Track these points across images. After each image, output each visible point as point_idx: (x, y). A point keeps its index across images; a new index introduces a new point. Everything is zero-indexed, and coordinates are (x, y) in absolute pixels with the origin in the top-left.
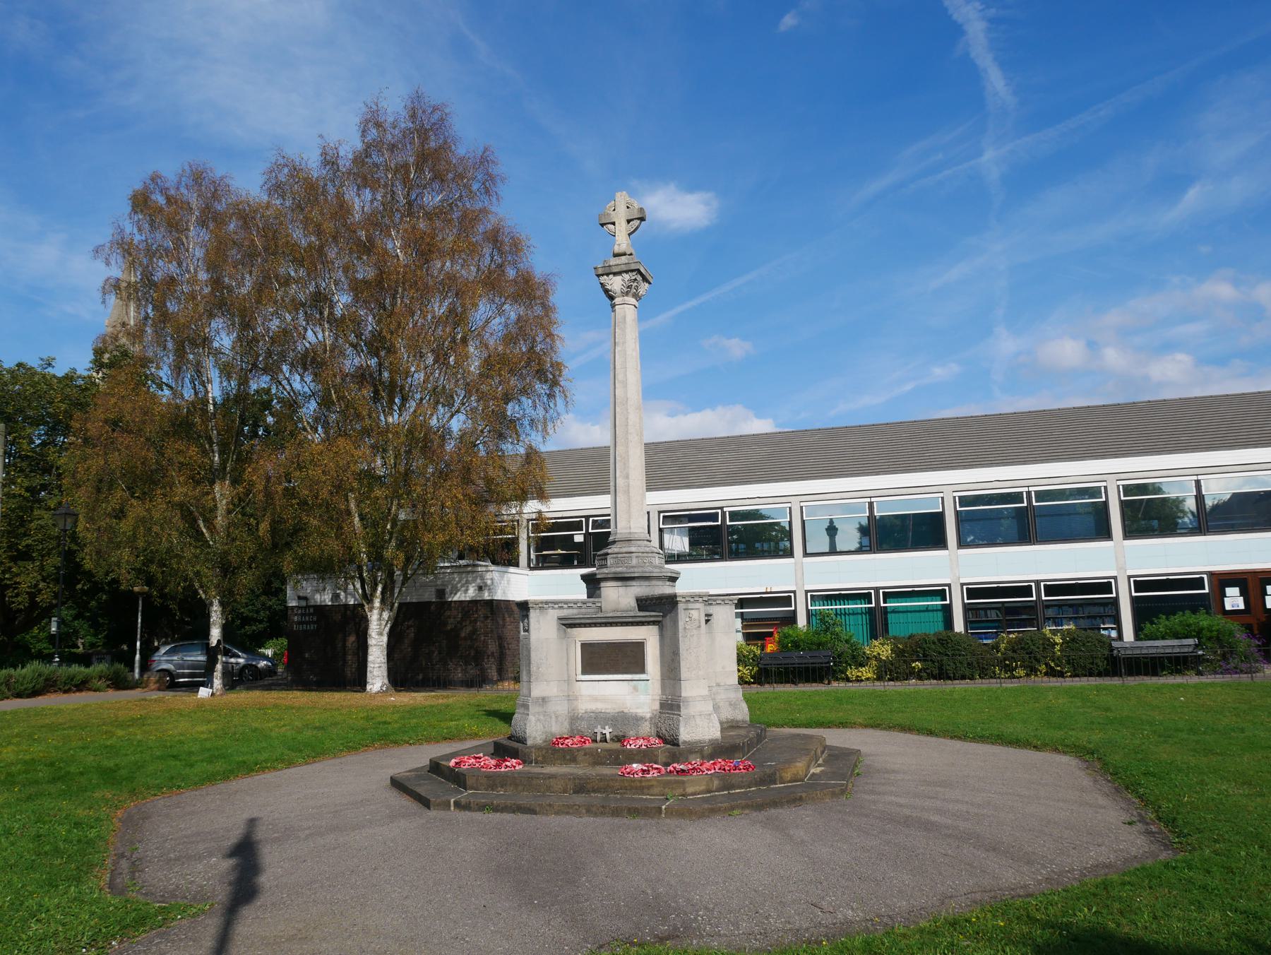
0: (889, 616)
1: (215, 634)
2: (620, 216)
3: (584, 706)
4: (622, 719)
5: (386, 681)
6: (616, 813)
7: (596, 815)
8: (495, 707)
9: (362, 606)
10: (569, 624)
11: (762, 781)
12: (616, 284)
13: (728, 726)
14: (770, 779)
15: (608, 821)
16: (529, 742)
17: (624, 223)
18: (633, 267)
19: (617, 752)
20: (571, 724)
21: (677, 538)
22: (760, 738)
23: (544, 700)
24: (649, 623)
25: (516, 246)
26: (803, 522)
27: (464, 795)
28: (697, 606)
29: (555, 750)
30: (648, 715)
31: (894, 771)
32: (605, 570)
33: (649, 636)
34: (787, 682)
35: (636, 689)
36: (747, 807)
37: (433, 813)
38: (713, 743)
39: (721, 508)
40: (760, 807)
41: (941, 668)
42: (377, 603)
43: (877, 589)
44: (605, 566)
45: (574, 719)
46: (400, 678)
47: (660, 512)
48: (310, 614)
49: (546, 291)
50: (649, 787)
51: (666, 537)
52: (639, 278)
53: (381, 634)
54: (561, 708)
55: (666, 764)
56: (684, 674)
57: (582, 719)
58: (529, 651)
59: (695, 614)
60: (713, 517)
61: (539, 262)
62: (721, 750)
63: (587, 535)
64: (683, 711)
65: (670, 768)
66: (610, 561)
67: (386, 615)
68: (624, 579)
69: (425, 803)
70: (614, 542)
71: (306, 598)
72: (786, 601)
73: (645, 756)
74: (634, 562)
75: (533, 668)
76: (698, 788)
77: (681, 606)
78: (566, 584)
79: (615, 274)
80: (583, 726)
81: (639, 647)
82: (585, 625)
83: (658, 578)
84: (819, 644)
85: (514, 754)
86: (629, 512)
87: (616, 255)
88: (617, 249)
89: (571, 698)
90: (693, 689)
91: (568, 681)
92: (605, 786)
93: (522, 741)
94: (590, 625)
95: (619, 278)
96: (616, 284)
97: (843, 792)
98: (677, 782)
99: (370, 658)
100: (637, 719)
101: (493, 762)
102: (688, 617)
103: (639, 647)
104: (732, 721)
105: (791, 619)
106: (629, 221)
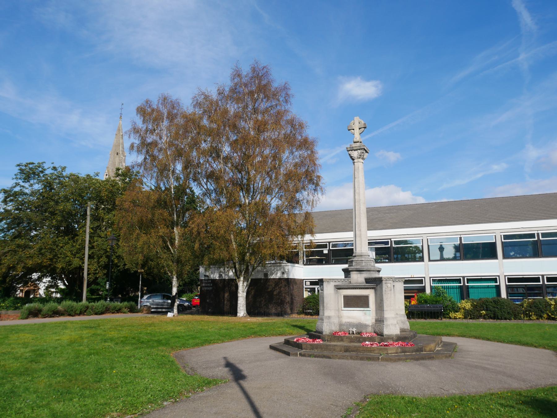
0: (470, 290)
1: (175, 291)
2: (356, 126)
3: (345, 320)
4: (360, 326)
5: (246, 312)
6: (362, 359)
7: (354, 360)
8: (294, 324)
9: (236, 280)
10: (338, 288)
11: (417, 351)
12: (355, 154)
13: (402, 330)
14: (420, 350)
15: (359, 362)
16: (324, 333)
17: (358, 129)
18: (362, 147)
19: (359, 338)
22: (415, 336)
23: (329, 317)
24: (370, 288)
25: (301, 126)
26: (428, 246)
27: (303, 351)
28: (390, 282)
29: (334, 336)
30: (371, 324)
31: (471, 351)
32: (352, 267)
33: (370, 293)
34: (422, 318)
35: (365, 314)
36: (412, 359)
37: (291, 357)
38: (397, 335)
39: (390, 239)
40: (417, 359)
41: (494, 314)
42: (242, 279)
43: (464, 277)
44: (352, 266)
45: (341, 325)
46: (252, 311)
48: (209, 283)
49: (313, 145)
50: (374, 350)
52: (364, 152)
53: (243, 292)
54: (336, 321)
55: (379, 343)
56: (385, 308)
57: (344, 325)
58: (323, 298)
59: (389, 285)
60: (387, 243)
61: (310, 133)
62: (399, 338)
63: (329, 250)
64: (385, 323)
65: (381, 344)
66: (354, 264)
67: (245, 284)
68: (360, 271)
69: (288, 354)
70: (355, 256)
71: (208, 276)
72: (421, 281)
73: (371, 339)
74: (364, 264)
75: (325, 305)
76: (393, 352)
77: (384, 282)
78: (333, 272)
79: (355, 150)
80: (344, 328)
81: (366, 298)
82: (345, 289)
83: (373, 271)
84: (436, 302)
85: (319, 338)
86: (361, 244)
87: (355, 142)
88: (355, 140)
89: (339, 317)
90: (389, 314)
91: (338, 310)
92: (356, 350)
93: (321, 333)
94: (347, 289)
95: (356, 152)
96: (355, 154)
97: (450, 356)
98: (384, 349)
99: (239, 302)
100: (366, 326)
101: (311, 340)
102: (386, 286)
103: (366, 298)
105: (423, 290)
106: (360, 129)
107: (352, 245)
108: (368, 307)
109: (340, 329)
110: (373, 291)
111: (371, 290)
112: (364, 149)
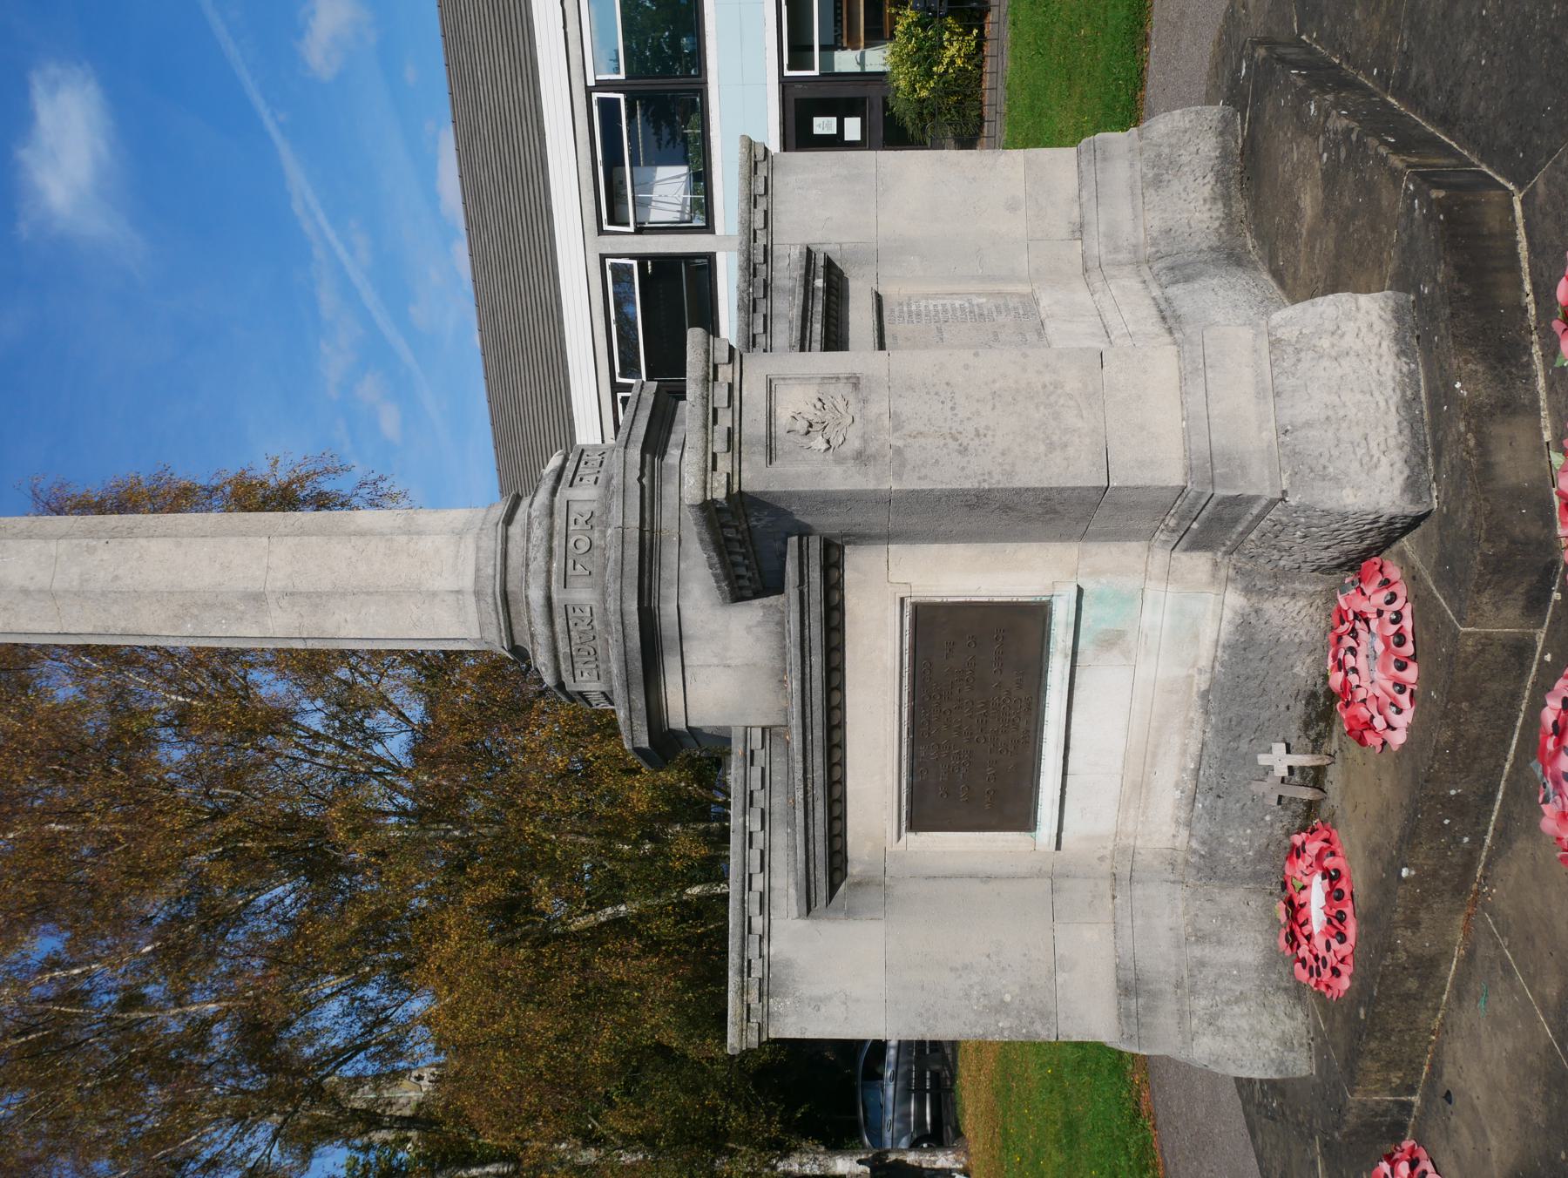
3: (1163, 825)
4: (1233, 696)
20: (1229, 878)
21: (659, 191)
23: (1131, 987)
28: (754, 391)
30: (1235, 599)
35: (1111, 640)
38: (1420, 333)
39: (589, 91)
47: (601, 232)
51: (656, 216)
54: (1164, 914)
60: (609, 108)
64: (1259, 482)
68: (652, 648)
77: (756, 477)
80: (1242, 841)
81: (934, 629)
89: (1123, 874)
100: (1246, 647)
103: (934, 629)
104: (1222, 178)
107: (621, 274)
108: (1035, 615)
109: (1256, 876)
110: (859, 566)
111: (849, 576)
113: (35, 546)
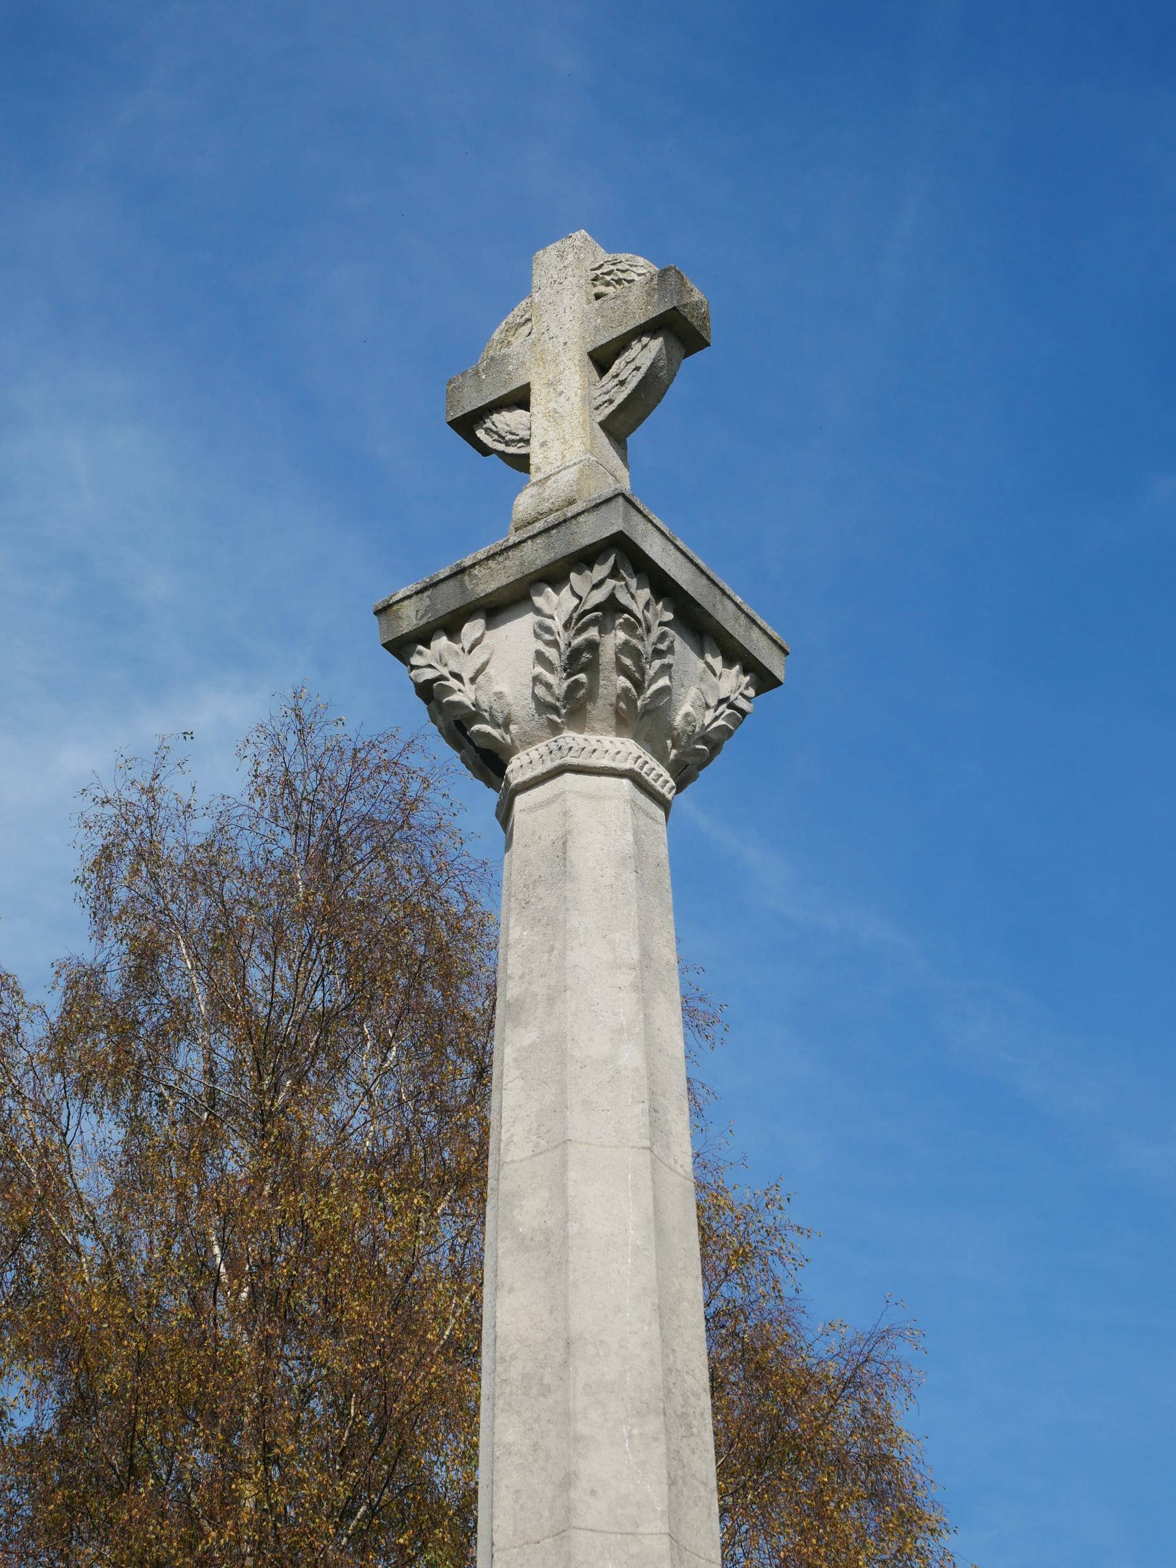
12: (503, 665)
52: (637, 598)
79: (496, 609)
112: (624, 552)
113: (655, 1492)
